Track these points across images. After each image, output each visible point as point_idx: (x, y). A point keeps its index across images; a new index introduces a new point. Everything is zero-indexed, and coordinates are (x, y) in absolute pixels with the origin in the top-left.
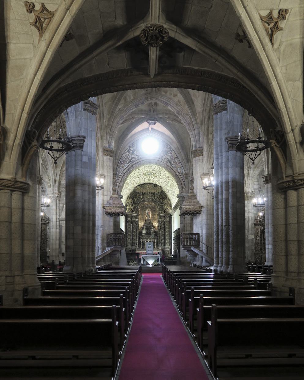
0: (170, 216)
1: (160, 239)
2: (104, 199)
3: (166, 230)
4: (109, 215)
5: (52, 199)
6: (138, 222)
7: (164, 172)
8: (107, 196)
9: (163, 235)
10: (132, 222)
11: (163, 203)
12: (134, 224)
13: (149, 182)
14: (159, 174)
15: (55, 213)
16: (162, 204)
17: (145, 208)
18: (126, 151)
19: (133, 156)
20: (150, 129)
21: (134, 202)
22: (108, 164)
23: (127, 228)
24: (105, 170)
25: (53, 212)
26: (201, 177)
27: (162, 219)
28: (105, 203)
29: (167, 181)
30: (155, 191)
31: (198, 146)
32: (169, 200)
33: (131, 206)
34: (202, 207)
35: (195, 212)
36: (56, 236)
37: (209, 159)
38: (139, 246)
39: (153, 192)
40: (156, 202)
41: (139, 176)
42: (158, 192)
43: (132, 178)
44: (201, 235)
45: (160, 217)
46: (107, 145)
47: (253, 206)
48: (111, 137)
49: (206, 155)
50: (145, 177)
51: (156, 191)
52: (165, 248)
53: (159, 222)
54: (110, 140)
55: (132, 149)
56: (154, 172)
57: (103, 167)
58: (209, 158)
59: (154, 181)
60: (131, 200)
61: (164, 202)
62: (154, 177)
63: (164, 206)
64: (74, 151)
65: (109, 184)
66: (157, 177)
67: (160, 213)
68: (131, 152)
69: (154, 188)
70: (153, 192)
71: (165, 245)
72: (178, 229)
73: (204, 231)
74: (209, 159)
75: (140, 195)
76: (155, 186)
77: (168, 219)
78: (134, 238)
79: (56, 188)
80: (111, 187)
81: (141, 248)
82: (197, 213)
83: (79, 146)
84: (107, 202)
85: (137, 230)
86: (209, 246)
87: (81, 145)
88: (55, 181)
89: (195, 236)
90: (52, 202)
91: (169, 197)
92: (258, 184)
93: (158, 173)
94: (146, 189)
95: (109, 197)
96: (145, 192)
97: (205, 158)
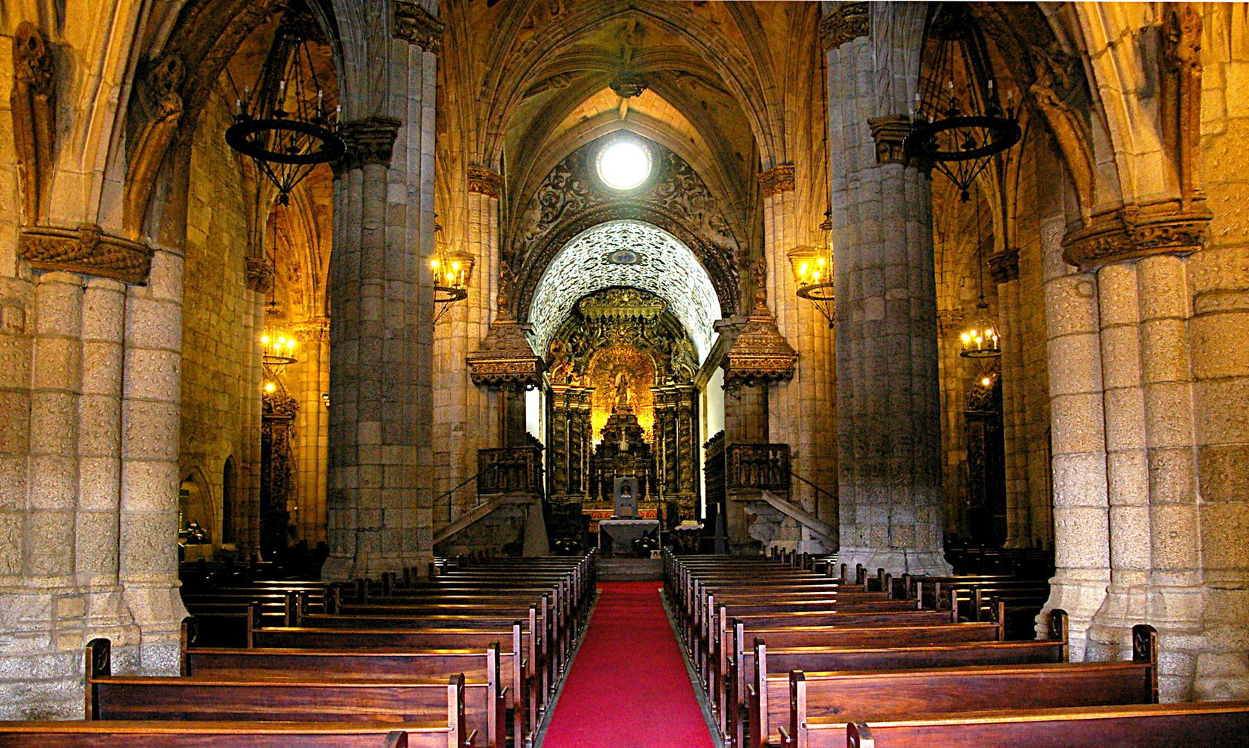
0: (694, 393)
1: (661, 468)
2: (470, 335)
4: (485, 388)
5: (306, 339)
7: (671, 250)
8: (479, 323)
10: (569, 416)
12: (576, 419)
14: (653, 257)
15: (313, 385)
16: (666, 353)
18: (547, 182)
19: (569, 197)
20: (624, 109)
22: (484, 221)
23: (552, 430)
24: (473, 237)
25: (308, 382)
26: (790, 260)
27: (666, 402)
28: (473, 347)
29: (683, 279)
30: (644, 313)
31: (779, 160)
32: (691, 342)
34: (797, 356)
35: (773, 373)
36: (317, 459)
37: (814, 203)
38: (593, 491)
39: (637, 316)
40: (646, 347)
41: (589, 265)
42: (652, 314)
43: (566, 271)
44: (793, 450)
45: (661, 398)
46: (479, 158)
47: (962, 355)
48: (494, 131)
49: (806, 190)
50: (612, 267)
51: (649, 311)
53: (657, 411)
54: (491, 144)
55: (566, 175)
56: (638, 249)
57: (466, 231)
58: (815, 199)
59: (638, 279)
62: (638, 267)
64: (361, 168)
65: (484, 285)
66: (650, 266)
67: (660, 383)
68: (562, 185)
70: (637, 316)
71: (676, 490)
72: (720, 435)
73: (805, 439)
74: (814, 203)
76: (646, 295)
79: (318, 304)
80: (494, 295)
81: (600, 498)
82: (780, 378)
83: (377, 152)
84: (481, 345)
85: (585, 441)
86: (820, 486)
87: (386, 147)
88: (316, 281)
89: (775, 455)
90: (305, 348)
91: (689, 332)
92: (976, 287)
93: (651, 252)
95: (487, 326)
96: (611, 316)
97: (804, 197)
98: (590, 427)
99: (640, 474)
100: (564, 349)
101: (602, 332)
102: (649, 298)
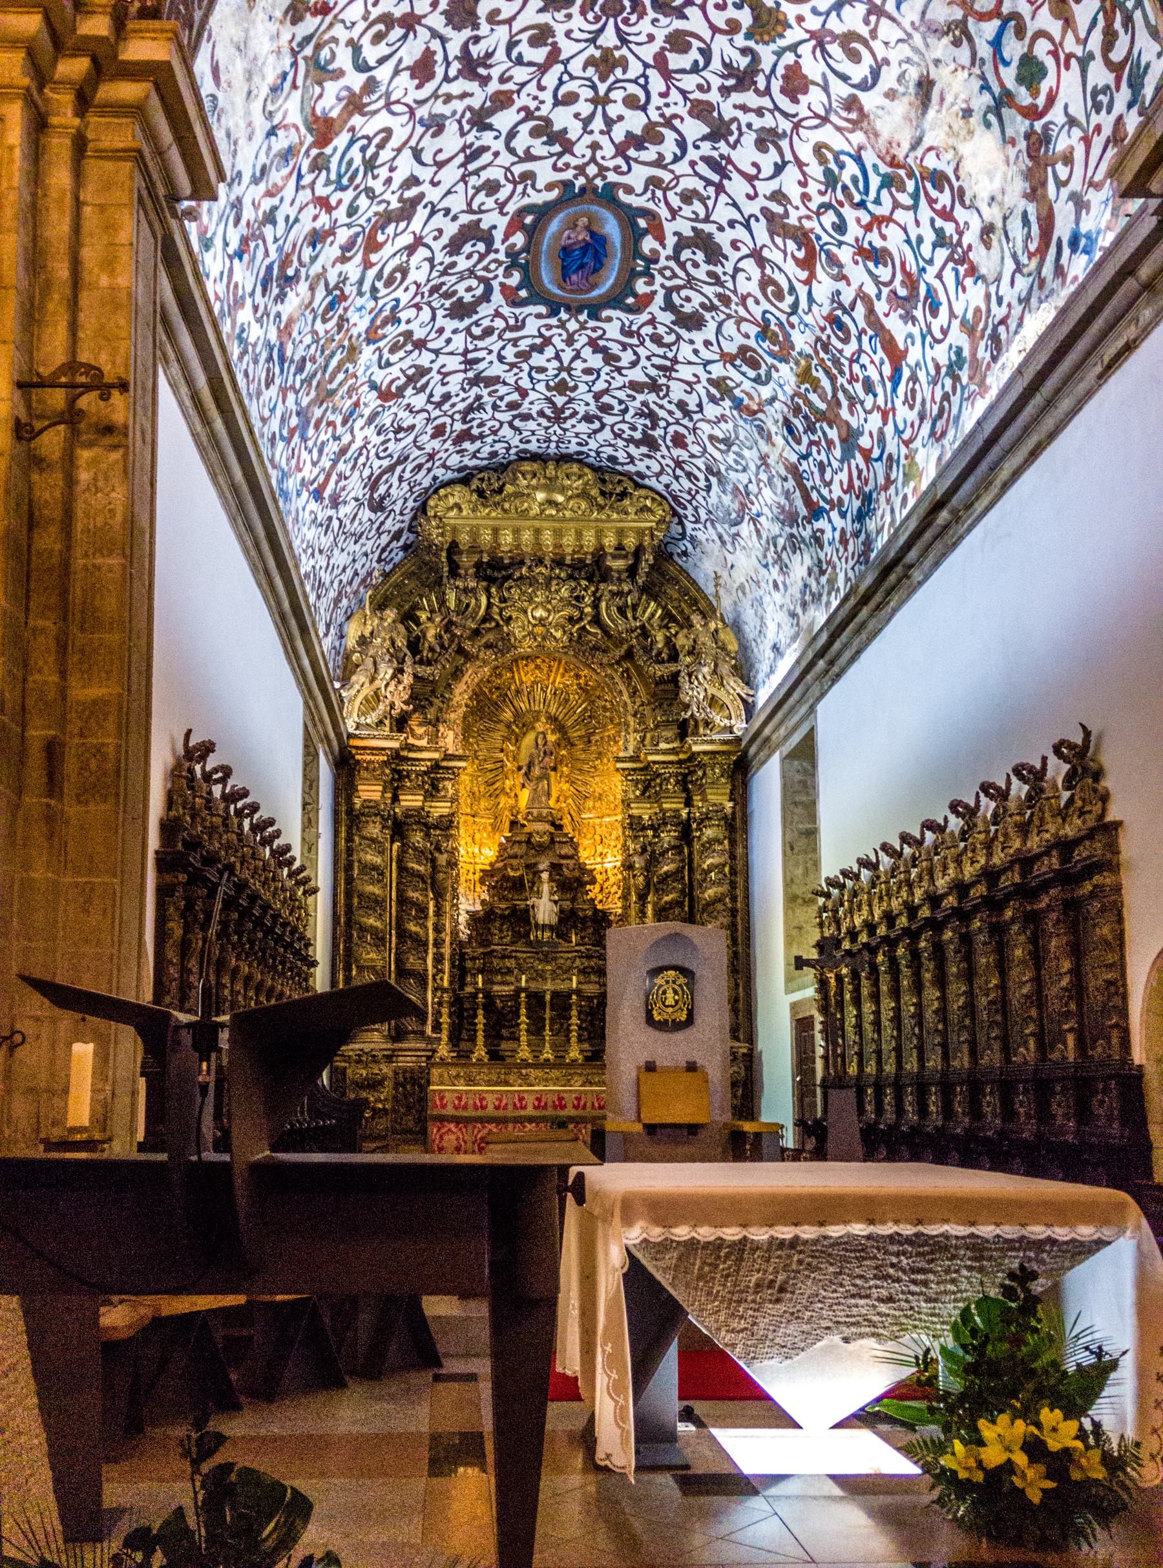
10: (399, 828)
12: (417, 838)
13: (553, 449)
17: (508, 715)
21: (414, 646)
27: (657, 799)
33: (385, 671)
42: (630, 542)
60: (391, 614)
69: (601, 508)
75: (472, 584)
94: (524, 514)
98: (453, 864)
101: (489, 605)
102: (623, 495)
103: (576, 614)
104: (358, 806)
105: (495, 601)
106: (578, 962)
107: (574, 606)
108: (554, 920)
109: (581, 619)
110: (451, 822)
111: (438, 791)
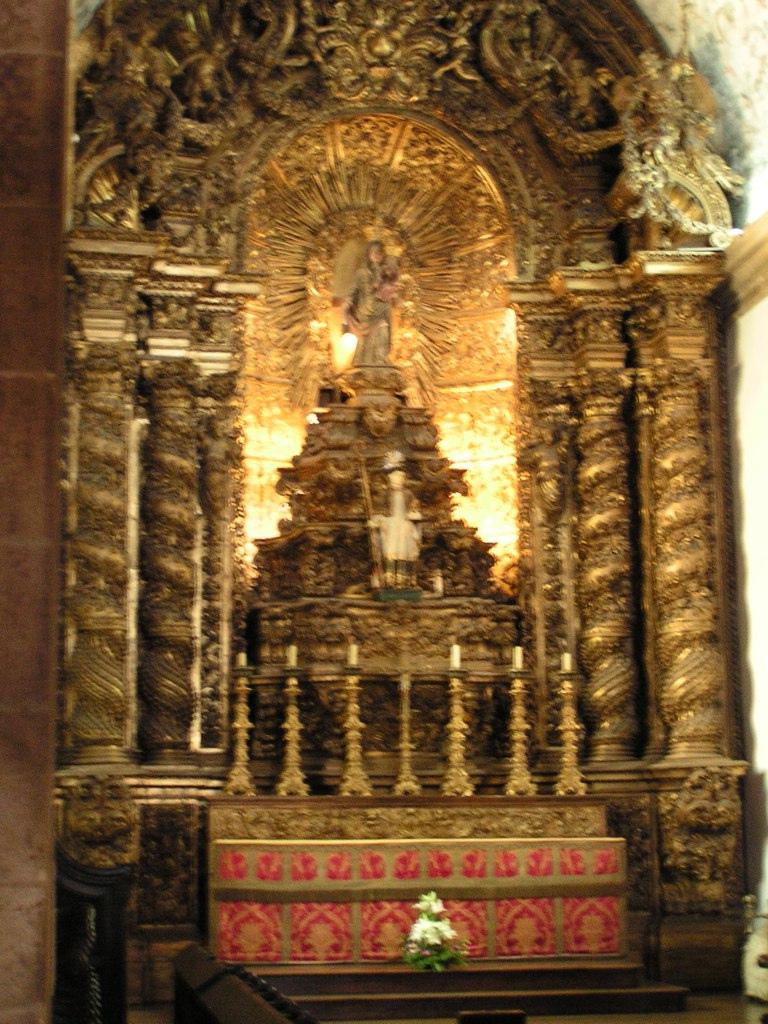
3: (671, 512)
6: (224, 387)
9: (614, 585)
10: (147, 391)
11: (608, 118)
12: (178, 408)
17: (314, 214)
52: (657, 782)
53: (536, 396)
61: (624, 99)
63: (629, 156)
77: (686, 347)
78: (170, 626)
81: (293, 779)
85: (211, 510)
98: (235, 457)
99: (483, 671)
100: (136, 69)
101: (301, 29)
103: (443, 48)
104: (82, 355)
105: (310, 21)
106: (456, 625)
107: (438, 35)
108: (414, 554)
109: (450, 57)
110: (232, 386)
111: (211, 334)
